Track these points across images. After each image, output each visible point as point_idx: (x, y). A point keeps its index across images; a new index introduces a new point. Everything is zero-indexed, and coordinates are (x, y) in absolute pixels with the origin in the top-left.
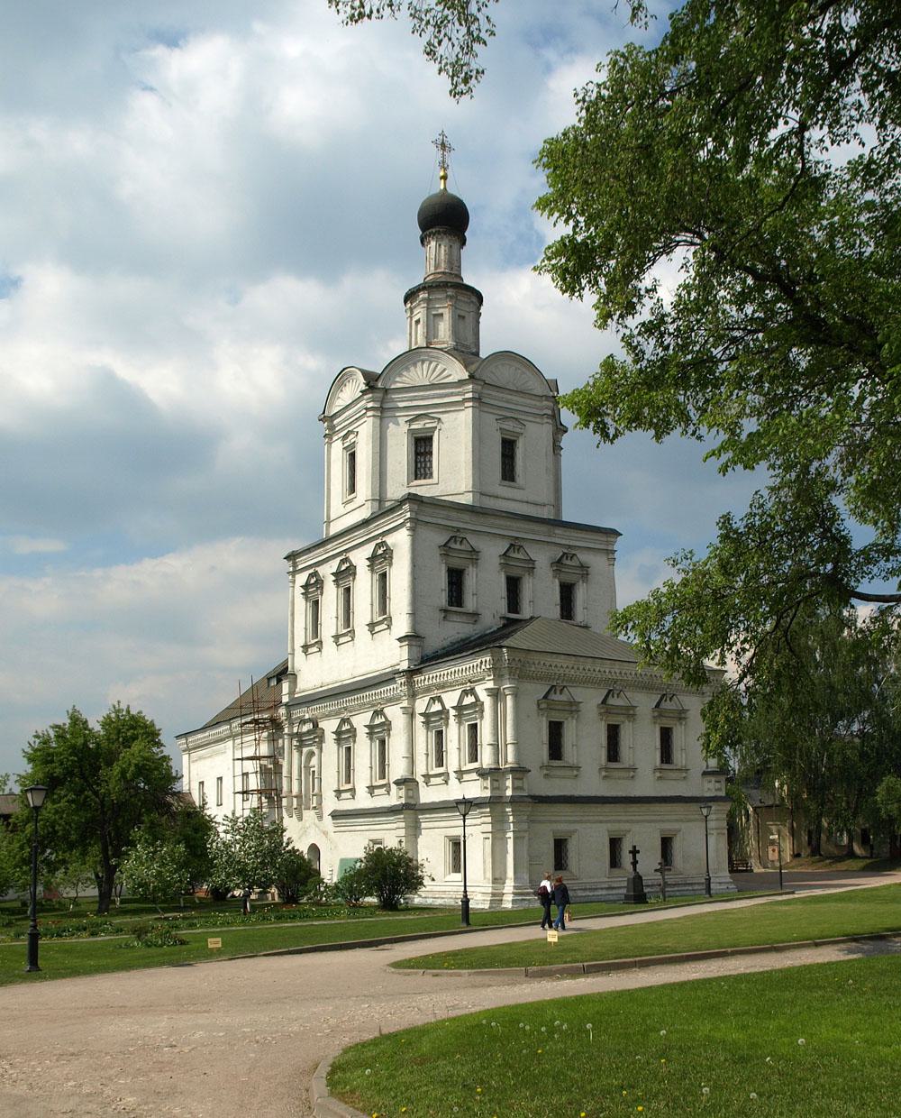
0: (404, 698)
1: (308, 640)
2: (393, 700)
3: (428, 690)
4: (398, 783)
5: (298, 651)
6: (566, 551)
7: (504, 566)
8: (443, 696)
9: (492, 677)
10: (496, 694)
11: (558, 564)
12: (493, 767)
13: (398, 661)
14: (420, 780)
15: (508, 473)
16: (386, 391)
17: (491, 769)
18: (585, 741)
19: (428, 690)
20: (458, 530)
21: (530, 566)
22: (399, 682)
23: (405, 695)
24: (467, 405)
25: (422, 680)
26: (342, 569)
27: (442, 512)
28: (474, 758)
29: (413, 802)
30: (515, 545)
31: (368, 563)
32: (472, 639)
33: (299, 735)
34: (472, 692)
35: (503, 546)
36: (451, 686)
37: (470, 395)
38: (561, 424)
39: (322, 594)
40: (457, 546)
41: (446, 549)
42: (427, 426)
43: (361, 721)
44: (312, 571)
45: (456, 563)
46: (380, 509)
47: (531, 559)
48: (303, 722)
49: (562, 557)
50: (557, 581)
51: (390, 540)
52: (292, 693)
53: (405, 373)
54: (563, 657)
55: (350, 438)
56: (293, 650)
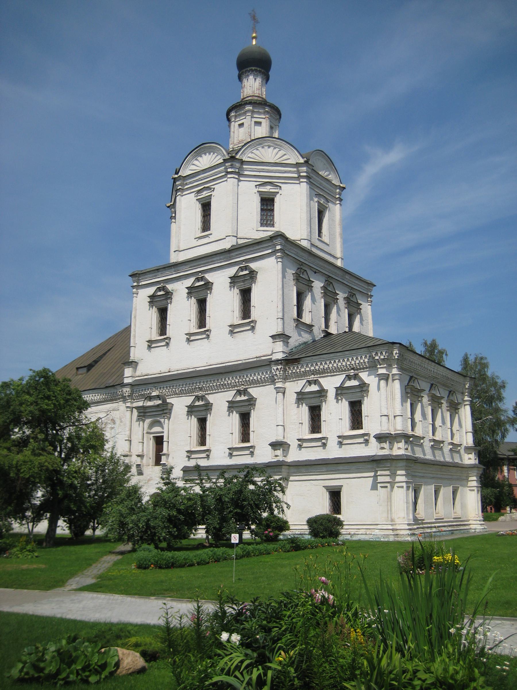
8: (321, 380)
13: (270, 353)
16: (242, 162)
20: (302, 264)
24: (302, 180)
26: (196, 285)
32: (309, 343)
36: (331, 372)
37: (305, 174)
42: (271, 190)
53: (260, 149)
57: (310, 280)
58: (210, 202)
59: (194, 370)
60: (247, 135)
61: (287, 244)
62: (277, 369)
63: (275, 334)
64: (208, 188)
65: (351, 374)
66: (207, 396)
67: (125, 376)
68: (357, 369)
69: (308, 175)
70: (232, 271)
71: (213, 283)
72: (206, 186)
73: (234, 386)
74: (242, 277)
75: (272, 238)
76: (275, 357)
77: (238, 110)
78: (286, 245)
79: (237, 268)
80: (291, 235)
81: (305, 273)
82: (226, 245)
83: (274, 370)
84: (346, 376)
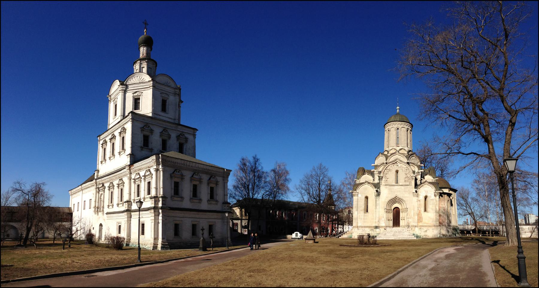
0: (128, 174)
2: (125, 175)
3: (135, 171)
4: (125, 202)
5: (100, 163)
6: (181, 133)
7: (161, 136)
9: (156, 165)
10: (157, 170)
11: (178, 137)
12: (155, 196)
14: (132, 201)
15: (164, 109)
17: (154, 197)
18: (186, 189)
19: (135, 171)
21: (169, 137)
22: (127, 169)
28: (149, 193)
29: (130, 209)
30: (165, 130)
31: (119, 134)
33: (99, 188)
34: (149, 170)
35: (161, 130)
38: (181, 100)
39: (106, 146)
40: (147, 128)
41: (142, 129)
43: (116, 183)
45: (147, 133)
46: (123, 117)
47: (169, 134)
48: (100, 184)
49: (180, 135)
50: (178, 142)
51: (125, 126)
52: (97, 176)
54: (180, 160)
56: (99, 163)
81: (149, 127)
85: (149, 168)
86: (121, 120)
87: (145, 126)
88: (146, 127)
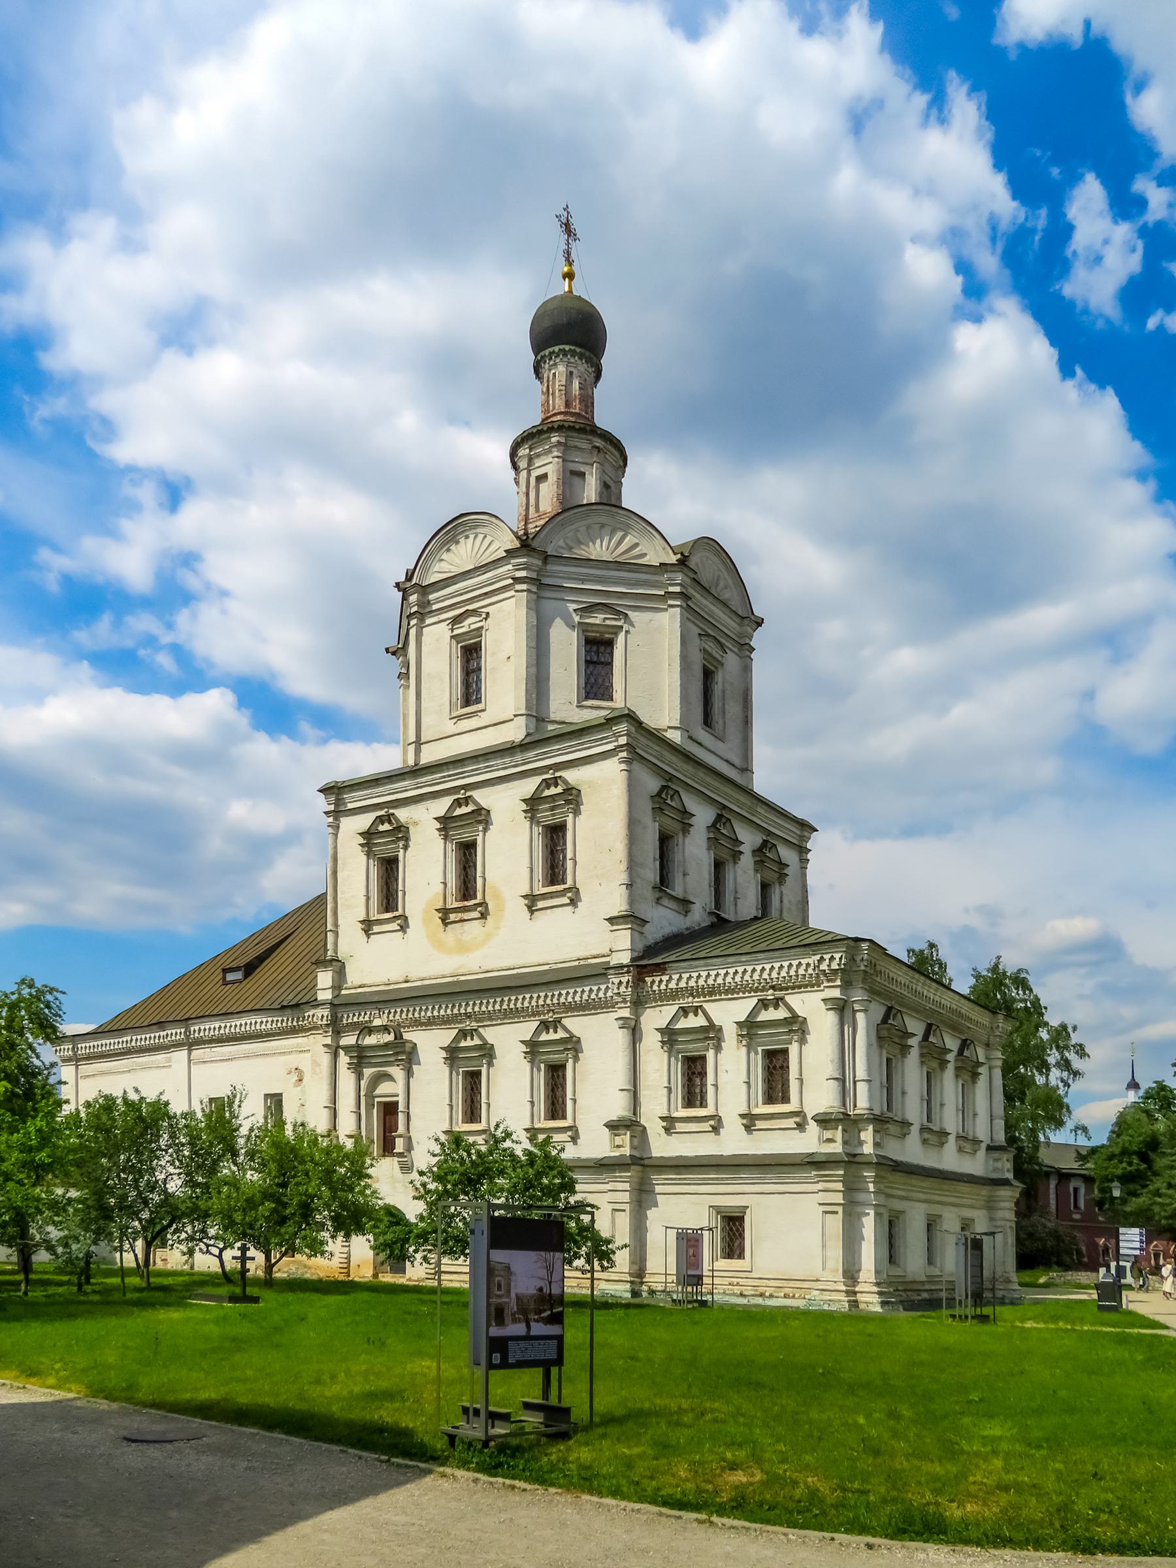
1: (371, 914)
3: (674, 995)
13: (607, 951)
19: (672, 995)
20: (671, 778)
22: (616, 981)
23: (625, 1001)
25: (657, 983)
27: (657, 748)
36: (727, 992)
39: (406, 848)
42: (608, 622)
44: (382, 813)
55: (466, 623)
57: (685, 812)
58: (481, 641)
59: (455, 979)
60: (555, 500)
61: (642, 735)
62: (620, 983)
63: (616, 914)
64: (474, 612)
65: (769, 998)
66: (480, 1029)
67: (319, 987)
68: (781, 989)
69: (684, 591)
70: (529, 786)
71: (489, 811)
72: (470, 607)
73: (534, 1015)
74: (550, 799)
75: (610, 722)
76: (615, 960)
77: (536, 443)
78: (639, 737)
79: (537, 780)
80: (650, 719)
81: (676, 797)
82: (516, 732)
83: (613, 983)
84: (759, 1000)
85: (779, 994)
86: (523, 747)
87: (663, 788)
88: (667, 794)
